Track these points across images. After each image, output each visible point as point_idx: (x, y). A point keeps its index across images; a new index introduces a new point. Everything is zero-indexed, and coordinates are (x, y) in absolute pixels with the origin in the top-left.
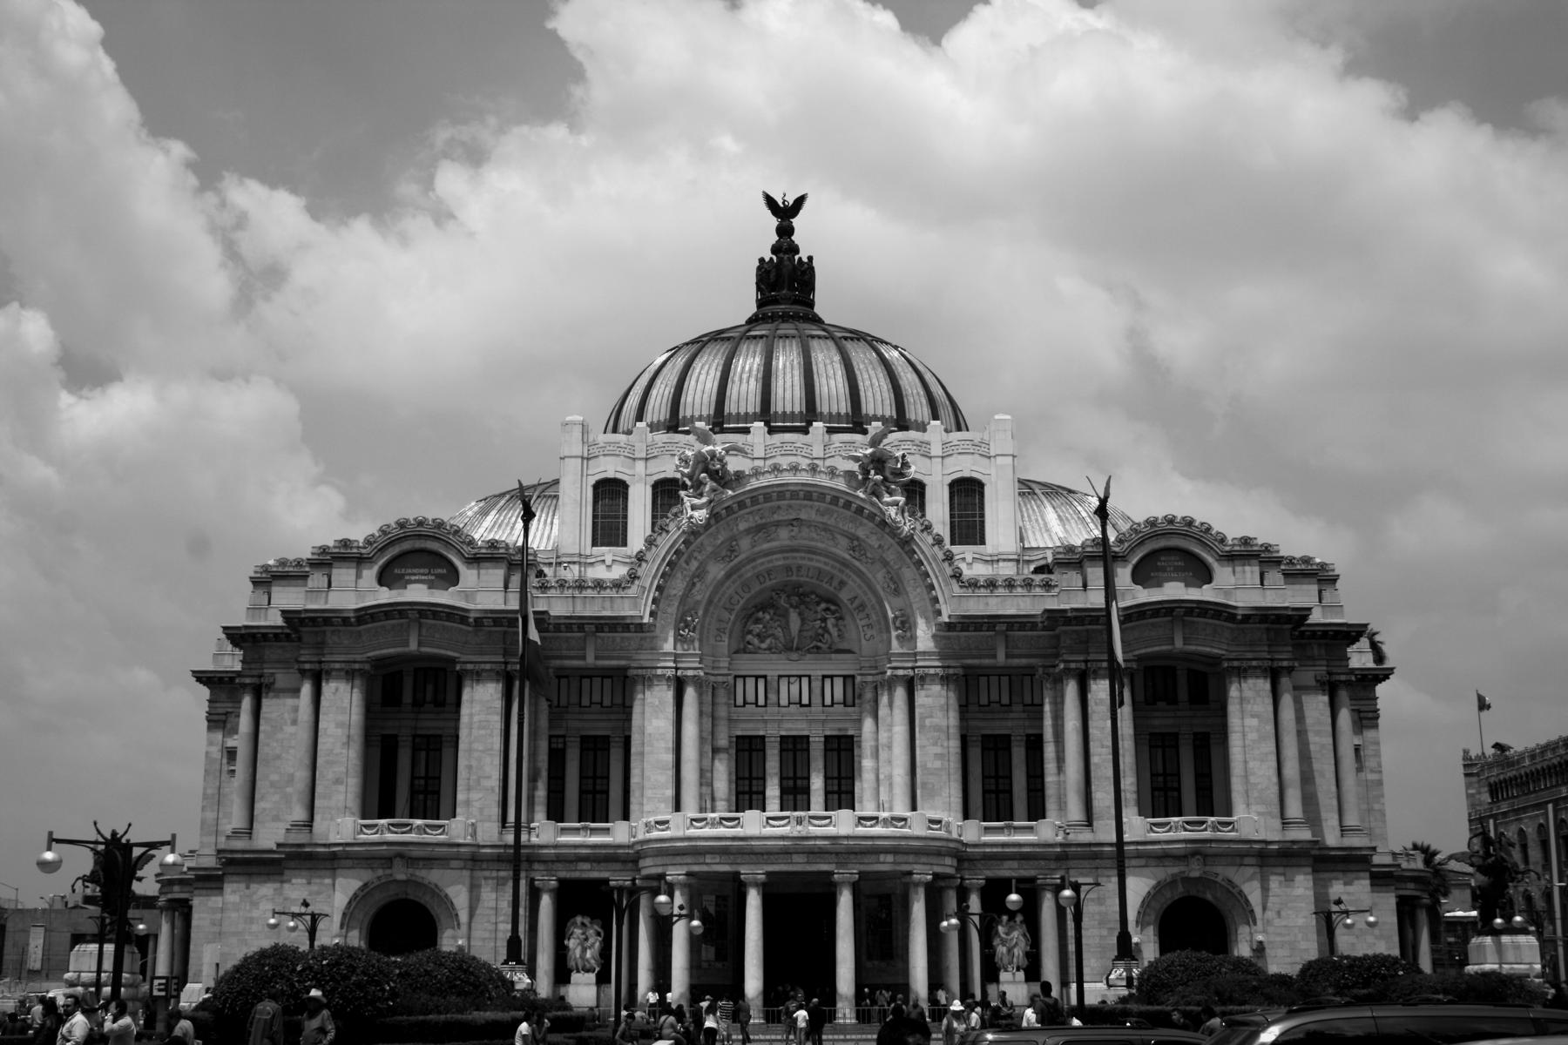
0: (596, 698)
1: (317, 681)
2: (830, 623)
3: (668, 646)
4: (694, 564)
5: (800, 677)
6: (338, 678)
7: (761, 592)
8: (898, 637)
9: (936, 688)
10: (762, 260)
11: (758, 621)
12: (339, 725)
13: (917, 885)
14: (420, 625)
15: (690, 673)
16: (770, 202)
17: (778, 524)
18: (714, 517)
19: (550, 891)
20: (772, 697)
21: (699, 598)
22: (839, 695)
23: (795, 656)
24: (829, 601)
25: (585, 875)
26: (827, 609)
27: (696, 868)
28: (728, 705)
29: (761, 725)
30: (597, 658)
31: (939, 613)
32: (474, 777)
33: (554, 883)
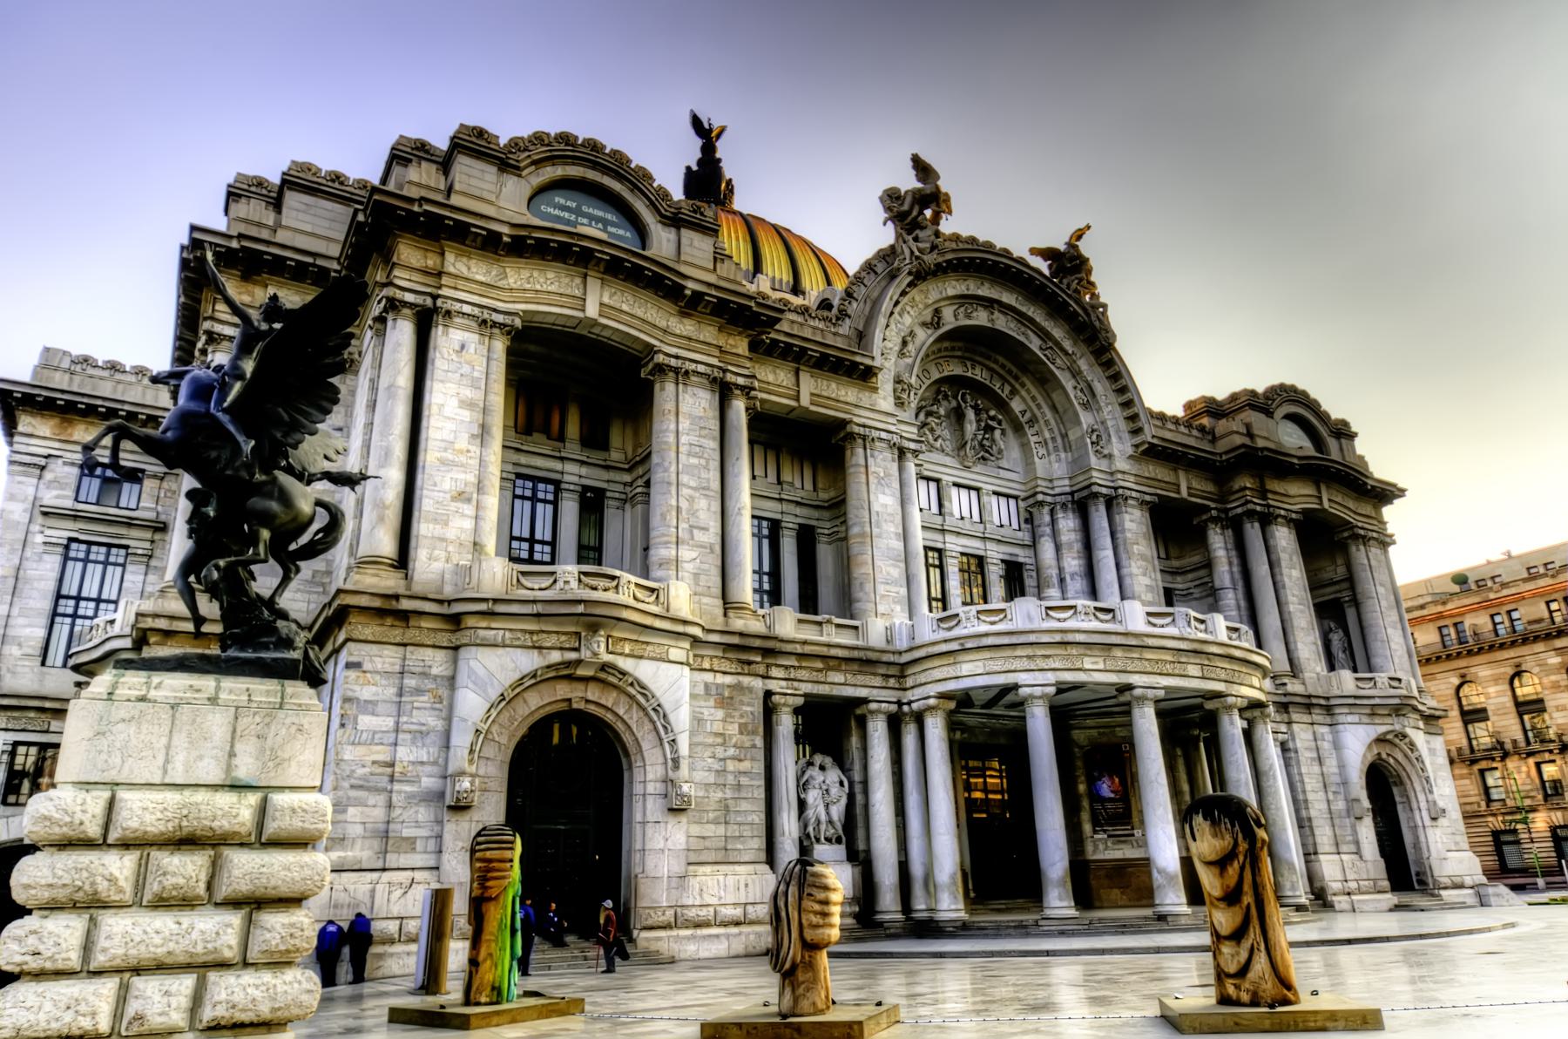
1: (425, 322)
2: (997, 433)
4: (908, 320)
5: (969, 488)
6: (467, 329)
9: (1137, 513)
10: (688, 168)
11: (929, 414)
12: (468, 405)
16: (696, 122)
18: (938, 265)
19: (797, 711)
26: (993, 418)
27: (1069, 677)
29: (938, 537)
31: (1137, 432)
32: (683, 525)
33: (800, 701)
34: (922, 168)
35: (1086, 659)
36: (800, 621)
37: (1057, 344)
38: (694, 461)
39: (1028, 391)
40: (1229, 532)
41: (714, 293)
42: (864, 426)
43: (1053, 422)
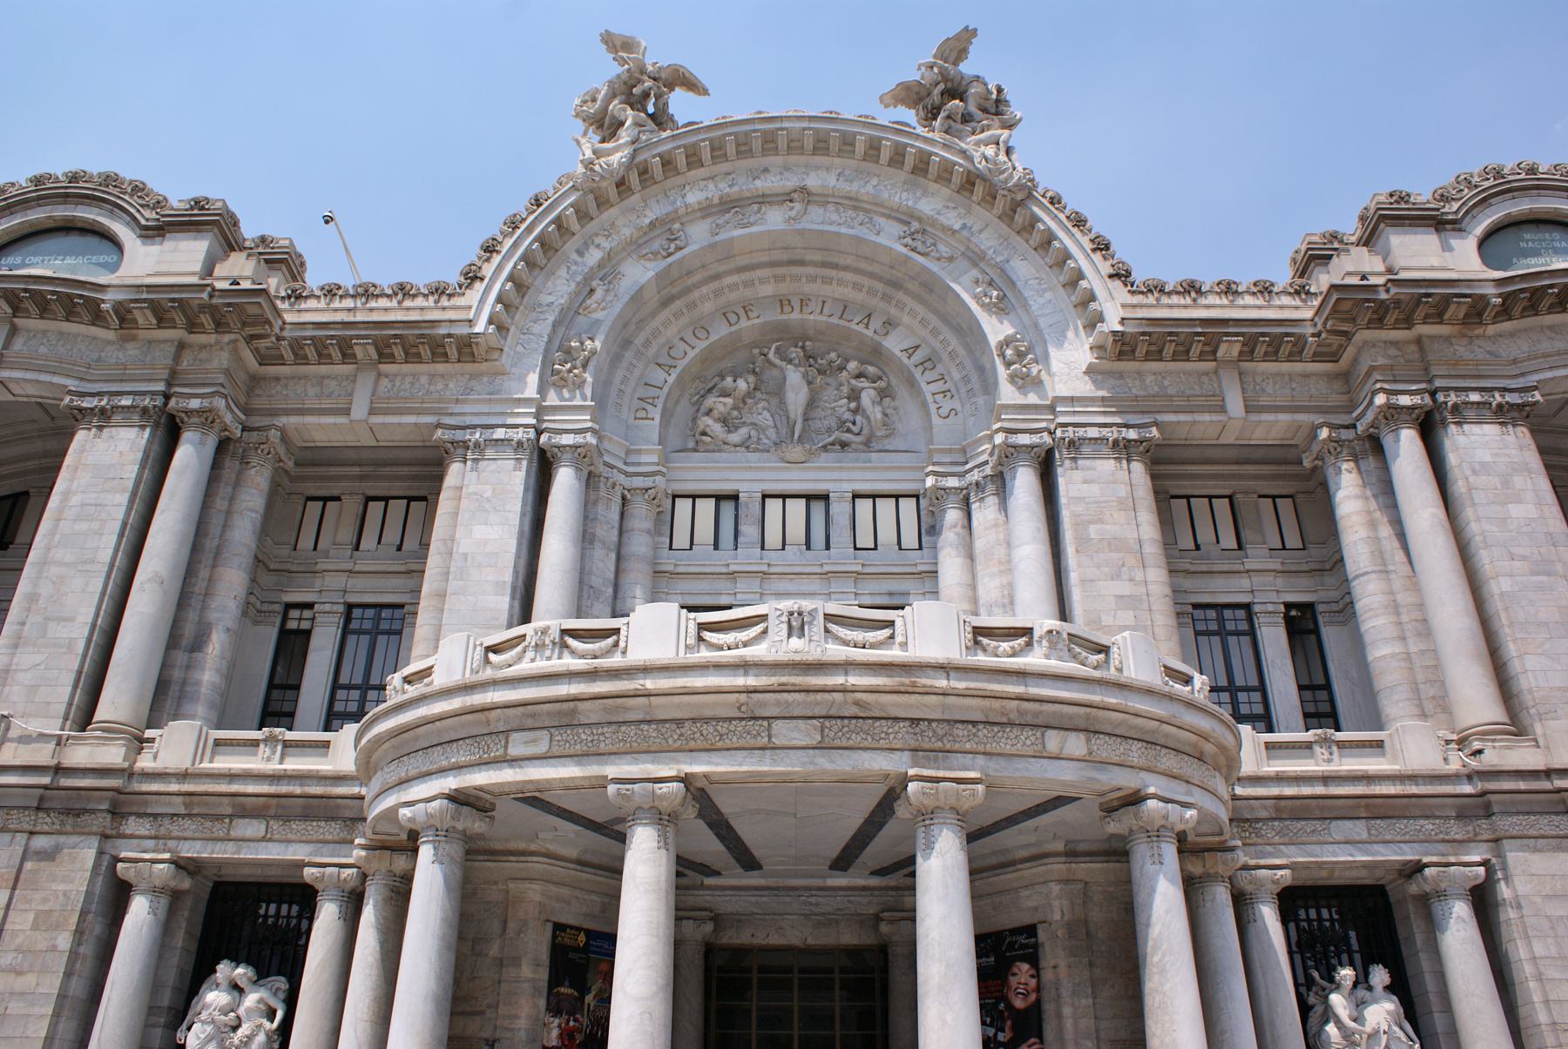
0: (392, 535)
2: (867, 397)
3: (531, 391)
7: (731, 345)
8: (1012, 378)
9: (1107, 466)
13: (1155, 834)
14: (14, 330)
15: (567, 440)
17: (763, 200)
20: (749, 531)
21: (599, 315)
22: (887, 533)
23: (796, 452)
24: (863, 362)
25: (247, 853)
26: (859, 376)
28: (656, 548)
29: (723, 585)
30: (372, 411)
34: (618, 45)
35: (515, 736)
36: (218, 743)
37: (933, 222)
38: (82, 526)
39: (911, 313)
40: (1370, 463)
41: (144, 296)
42: (468, 427)
43: (961, 352)
